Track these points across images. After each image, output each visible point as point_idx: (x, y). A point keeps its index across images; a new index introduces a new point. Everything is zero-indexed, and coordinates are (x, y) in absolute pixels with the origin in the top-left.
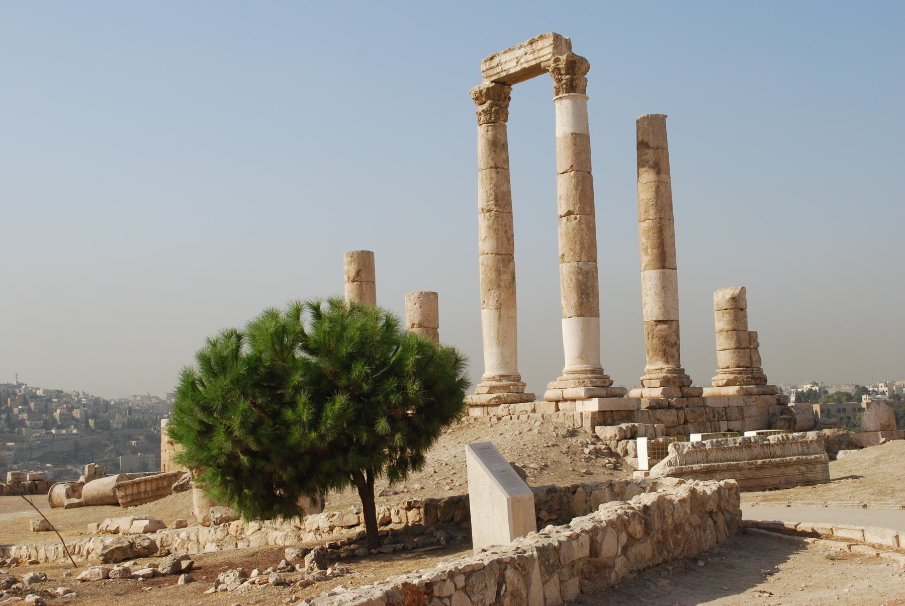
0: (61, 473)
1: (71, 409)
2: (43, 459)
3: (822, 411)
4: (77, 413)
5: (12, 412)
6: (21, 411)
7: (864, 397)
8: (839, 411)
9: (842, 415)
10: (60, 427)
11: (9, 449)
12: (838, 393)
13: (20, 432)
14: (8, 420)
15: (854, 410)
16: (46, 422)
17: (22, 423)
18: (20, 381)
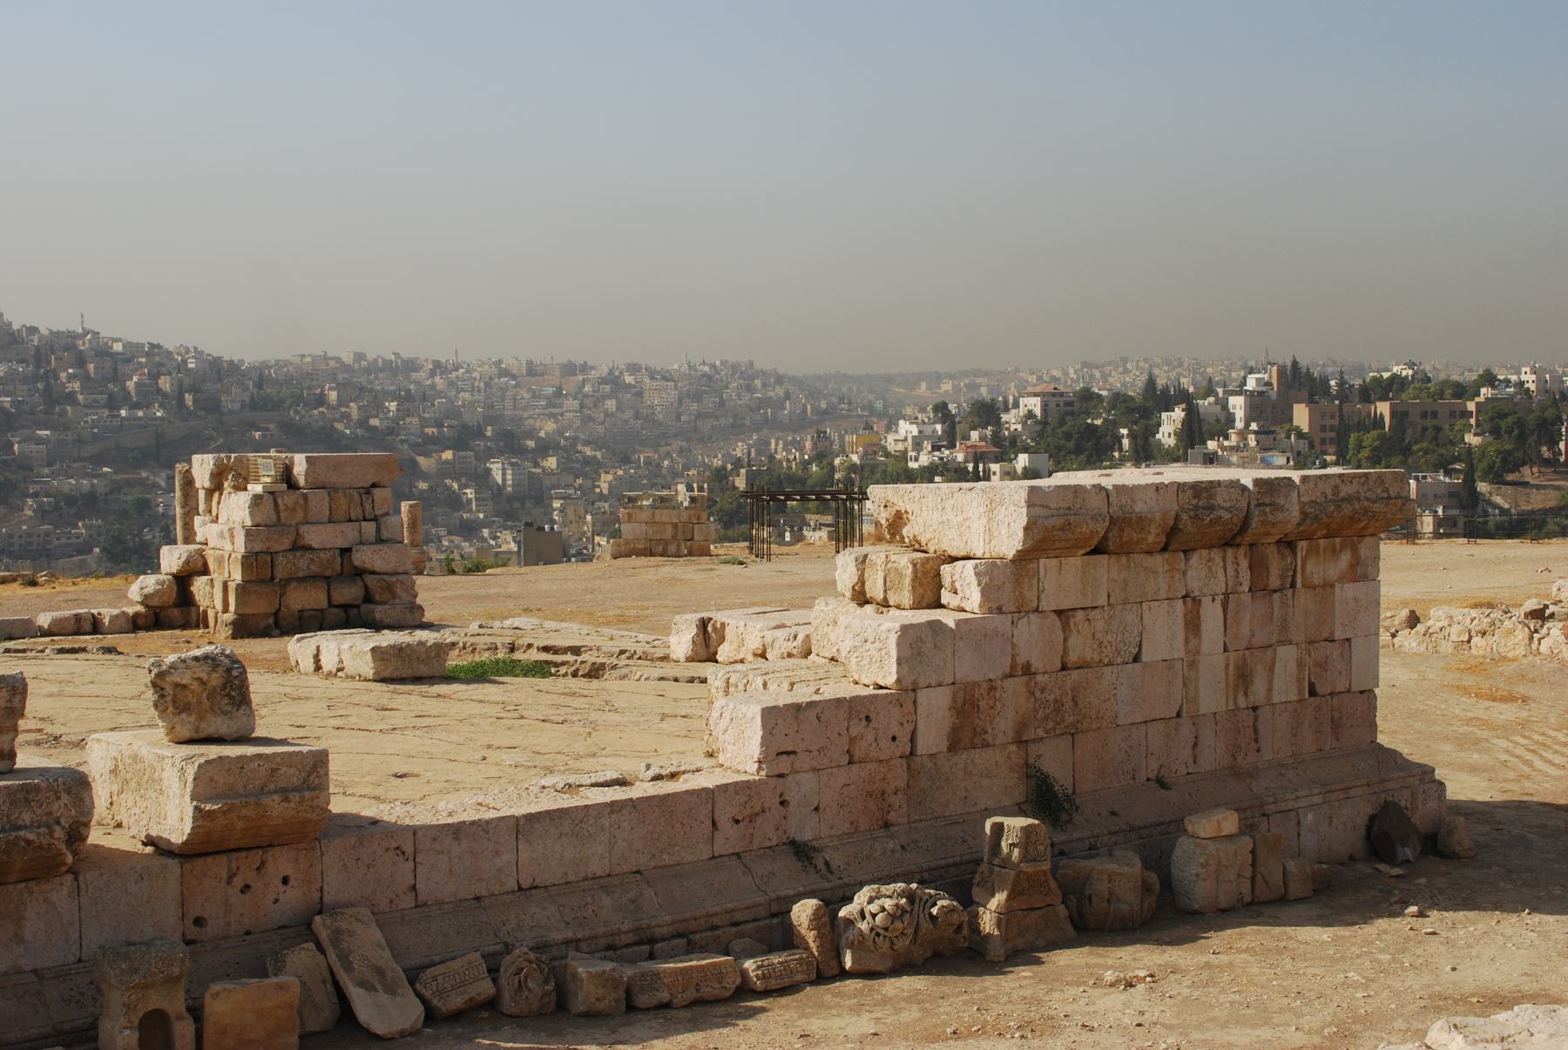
0: (128, 483)
1: (155, 376)
2: (98, 460)
3: (1393, 414)
4: (165, 383)
5: (57, 378)
6: (71, 378)
7: (1483, 390)
8: (1424, 415)
9: (1429, 422)
10: (136, 406)
11: (40, 441)
12: (1446, 382)
13: (63, 413)
14: (48, 389)
15: (1452, 414)
16: (111, 397)
17: (71, 398)
18: (88, 327)
